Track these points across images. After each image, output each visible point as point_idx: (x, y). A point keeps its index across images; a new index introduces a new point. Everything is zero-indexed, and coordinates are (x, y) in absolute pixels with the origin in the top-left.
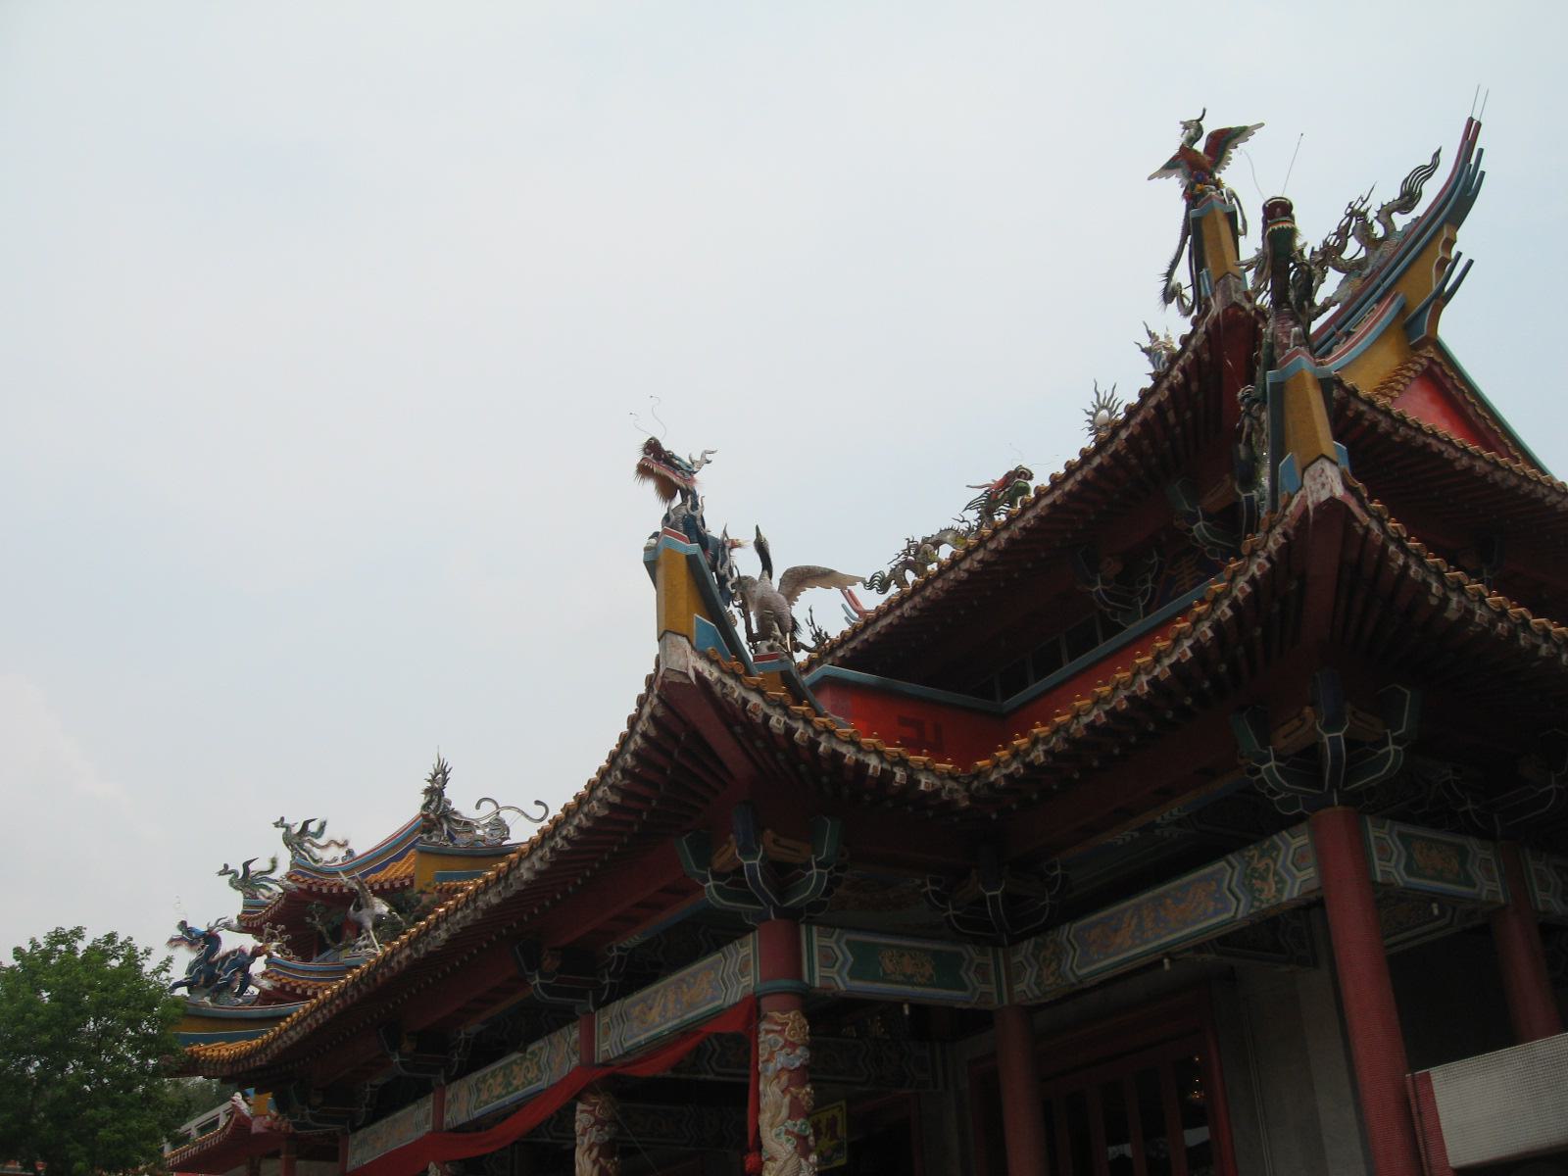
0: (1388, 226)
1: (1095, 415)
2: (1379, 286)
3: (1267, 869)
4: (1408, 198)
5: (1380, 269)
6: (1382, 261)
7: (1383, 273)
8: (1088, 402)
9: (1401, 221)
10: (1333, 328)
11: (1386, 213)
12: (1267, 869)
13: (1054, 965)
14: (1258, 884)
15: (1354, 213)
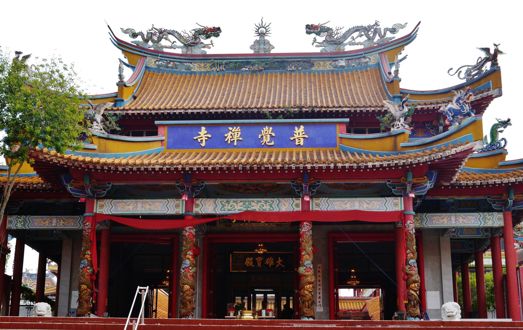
0: (385, 34)
1: (259, 28)
2: (381, 49)
3: (490, 219)
4: (393, 31)
5: (381, 45)
6: (382, 43)
7: (383, 47)
8: (258, 22)
9: (389, 35)
10: (362, 53)
11: (386, 30)
12: (490, 219)
13: (419, 221)
14: (487, 221)
15: (376, 24)
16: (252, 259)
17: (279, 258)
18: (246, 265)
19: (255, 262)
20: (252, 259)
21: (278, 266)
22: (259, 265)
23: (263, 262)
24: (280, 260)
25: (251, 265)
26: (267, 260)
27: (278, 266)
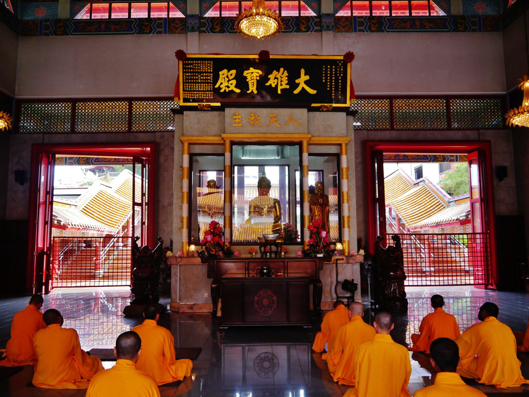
16: (234, 72)
17: (303, 71)
18: (219, 88)
19: (242, 82)
20: (234, 72)
21: (296, 92)
22: (253, 88)
23: (262, 82)
24: (304, 78)
25: (232, 88)
26: (271, 76)
27: (296, 92)
